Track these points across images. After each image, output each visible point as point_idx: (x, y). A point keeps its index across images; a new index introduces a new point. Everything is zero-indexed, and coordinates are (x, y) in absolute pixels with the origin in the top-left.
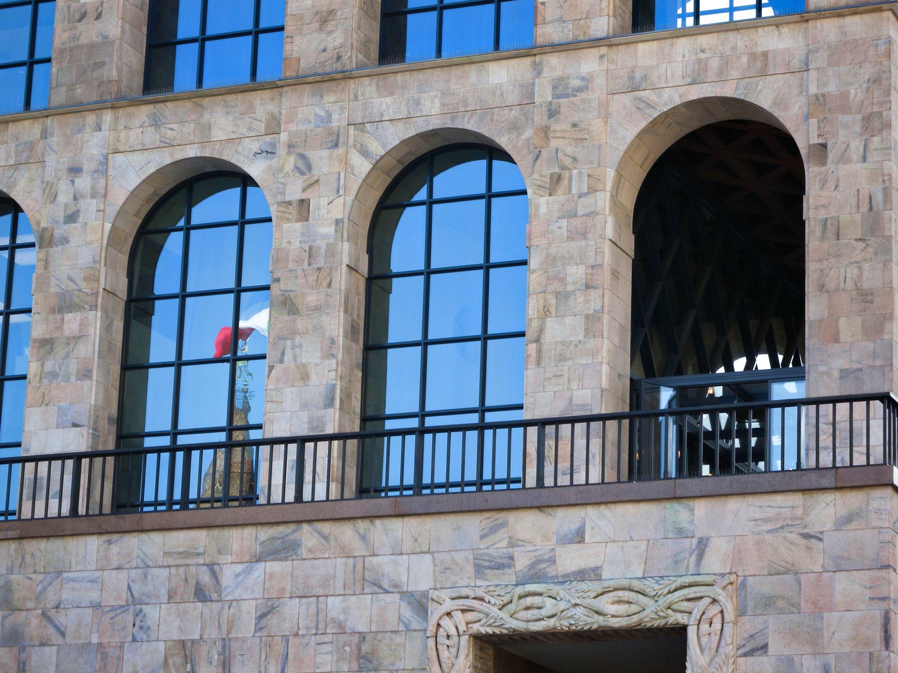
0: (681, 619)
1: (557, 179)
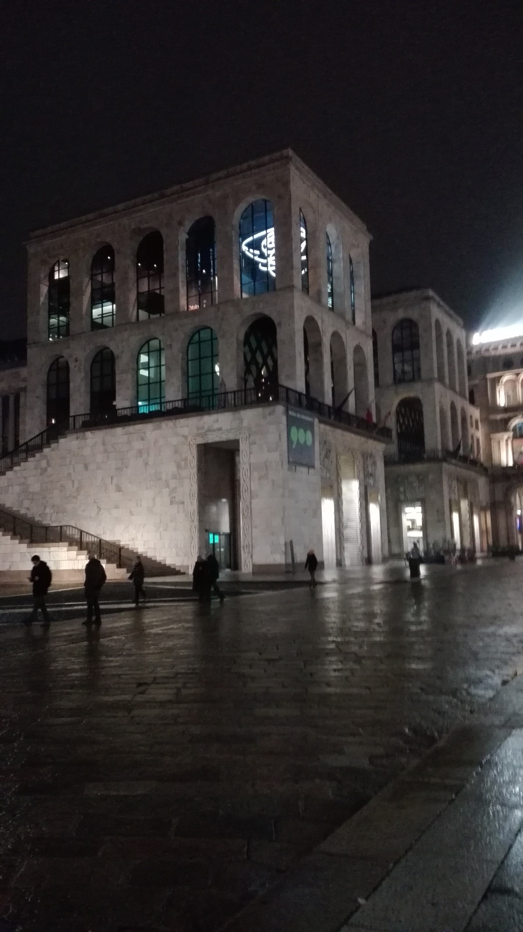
0: (237, 438)
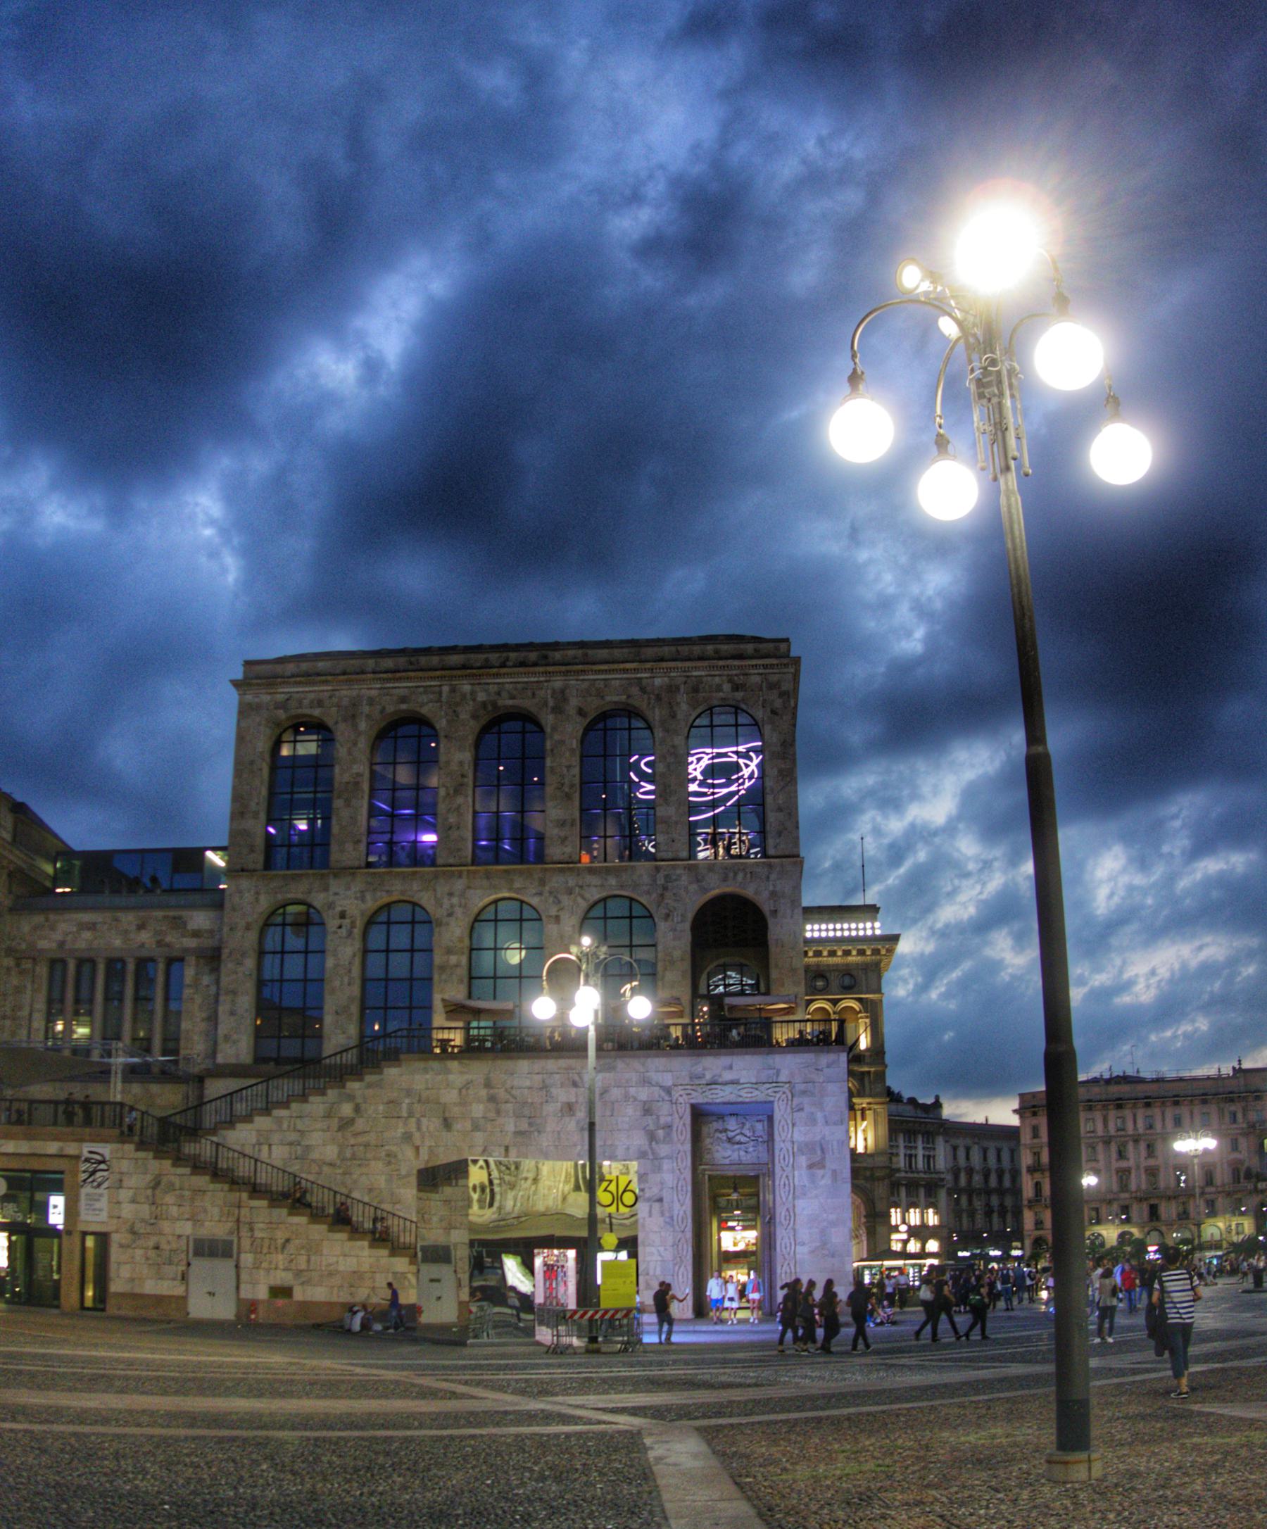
1: (667, 916)
